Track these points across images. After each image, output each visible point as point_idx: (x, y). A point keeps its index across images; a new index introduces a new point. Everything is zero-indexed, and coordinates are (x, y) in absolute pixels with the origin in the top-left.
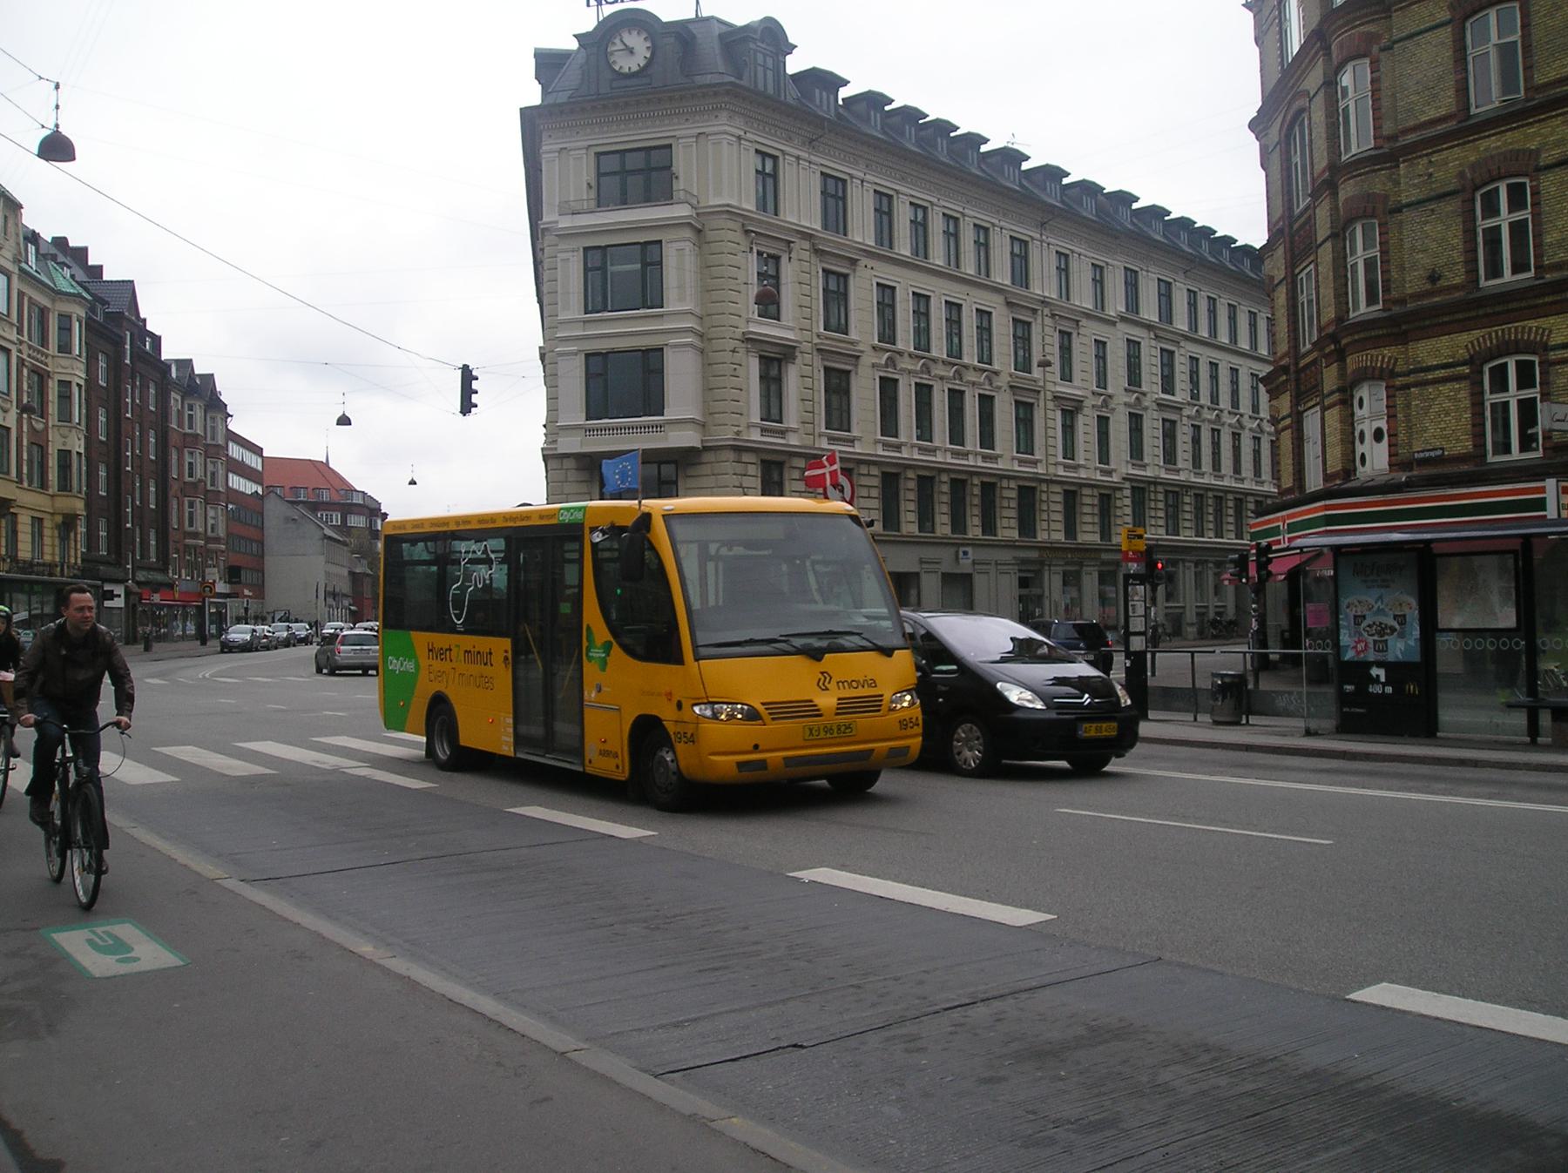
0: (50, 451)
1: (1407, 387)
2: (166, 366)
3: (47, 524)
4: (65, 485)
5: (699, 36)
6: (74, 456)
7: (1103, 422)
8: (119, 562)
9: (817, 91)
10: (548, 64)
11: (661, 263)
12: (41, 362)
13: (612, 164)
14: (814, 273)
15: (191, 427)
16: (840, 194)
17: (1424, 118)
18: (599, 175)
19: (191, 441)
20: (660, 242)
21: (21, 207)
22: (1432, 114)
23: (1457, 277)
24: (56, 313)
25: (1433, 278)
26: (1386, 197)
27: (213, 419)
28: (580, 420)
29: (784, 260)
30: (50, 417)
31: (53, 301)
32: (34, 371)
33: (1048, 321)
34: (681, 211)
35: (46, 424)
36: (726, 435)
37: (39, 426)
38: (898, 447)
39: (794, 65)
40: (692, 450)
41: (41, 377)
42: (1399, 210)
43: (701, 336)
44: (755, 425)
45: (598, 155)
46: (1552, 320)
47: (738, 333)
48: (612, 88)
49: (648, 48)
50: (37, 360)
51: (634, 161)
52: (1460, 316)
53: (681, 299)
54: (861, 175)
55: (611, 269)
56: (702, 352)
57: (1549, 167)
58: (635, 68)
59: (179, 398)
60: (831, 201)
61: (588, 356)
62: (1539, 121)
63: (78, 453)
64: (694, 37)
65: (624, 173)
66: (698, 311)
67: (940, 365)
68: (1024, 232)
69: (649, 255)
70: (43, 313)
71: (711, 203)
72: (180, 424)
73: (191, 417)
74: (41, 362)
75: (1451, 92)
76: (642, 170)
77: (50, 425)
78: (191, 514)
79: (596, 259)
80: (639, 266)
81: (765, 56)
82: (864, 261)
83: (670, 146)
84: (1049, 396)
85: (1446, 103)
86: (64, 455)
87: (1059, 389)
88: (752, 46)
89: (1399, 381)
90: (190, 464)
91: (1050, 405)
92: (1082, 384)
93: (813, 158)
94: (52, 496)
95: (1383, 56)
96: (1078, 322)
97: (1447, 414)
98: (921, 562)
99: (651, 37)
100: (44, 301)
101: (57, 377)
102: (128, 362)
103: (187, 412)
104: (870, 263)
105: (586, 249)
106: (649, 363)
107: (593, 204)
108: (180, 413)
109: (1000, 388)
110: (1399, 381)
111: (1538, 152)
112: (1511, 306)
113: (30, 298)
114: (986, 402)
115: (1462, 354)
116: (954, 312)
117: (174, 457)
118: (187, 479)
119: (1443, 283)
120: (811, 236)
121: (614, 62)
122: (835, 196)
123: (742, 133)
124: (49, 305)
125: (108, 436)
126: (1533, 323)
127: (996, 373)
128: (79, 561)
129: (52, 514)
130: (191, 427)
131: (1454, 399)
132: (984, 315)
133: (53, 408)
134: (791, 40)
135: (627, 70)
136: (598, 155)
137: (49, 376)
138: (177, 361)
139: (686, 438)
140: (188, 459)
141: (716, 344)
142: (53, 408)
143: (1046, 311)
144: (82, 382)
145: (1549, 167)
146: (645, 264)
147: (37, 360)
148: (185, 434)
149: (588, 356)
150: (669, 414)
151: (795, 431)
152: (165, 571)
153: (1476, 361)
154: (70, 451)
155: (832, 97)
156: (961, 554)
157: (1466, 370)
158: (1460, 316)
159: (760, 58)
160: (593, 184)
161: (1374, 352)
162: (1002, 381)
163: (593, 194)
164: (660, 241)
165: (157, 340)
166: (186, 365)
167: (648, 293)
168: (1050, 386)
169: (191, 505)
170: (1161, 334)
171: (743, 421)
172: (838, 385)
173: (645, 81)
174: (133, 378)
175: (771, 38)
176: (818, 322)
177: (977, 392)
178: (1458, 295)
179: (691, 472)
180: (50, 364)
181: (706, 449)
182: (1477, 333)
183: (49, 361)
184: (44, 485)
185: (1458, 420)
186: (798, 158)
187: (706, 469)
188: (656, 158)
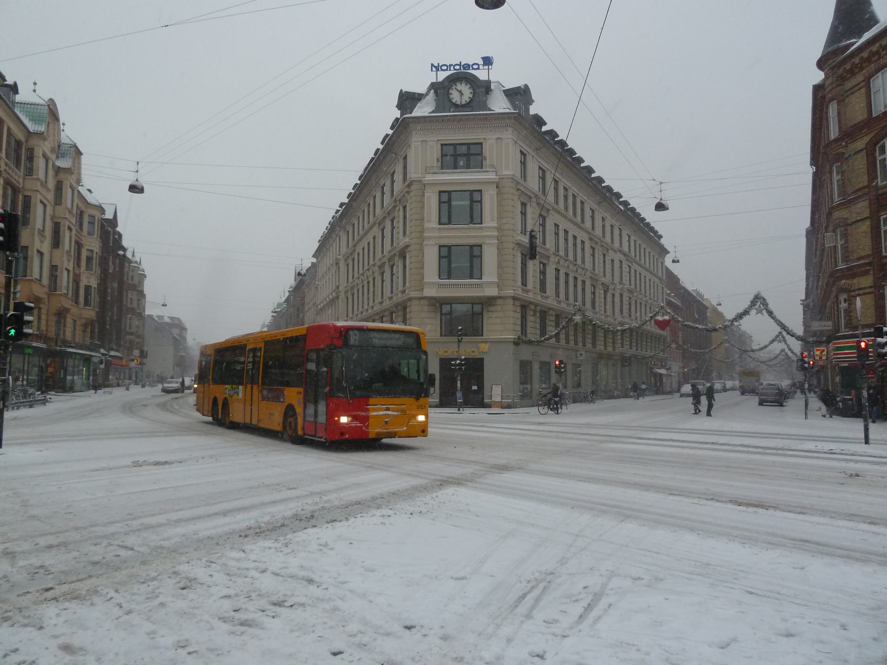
3: (78, 323)
4: (87, 303)
6: (93, 289)
7: (613, 295)
12: (80, 239)
13: (450, 150)
20: (481, 191)
21: (81, 154)
24: (88, 214)
28: (436, 279)
29: (528, 206)
33: (600, 249)
34: (492, 176)
35: (80, 271)
36: (510, 292)
37: (77, 272)
39: (533, 110)
41: (79, 245)
45: (442, 145)
49: (471, 93)
51: (463, 149)
53: (492, 220)
55: (453, 203)
58: (464, 102)
63: (95, 288)
65: (456, 156)
69: (474, 197)
70: (81, 214)
72: (128, 279)
76: (465, 154)
79: (445, 197)
80: (468, 202)
83: (481, 144)
84: (600, 283)
86: (88, 288)
90: (131, 299)
91: (601, 287)
92: (607, 280)
96: (608, 250)
99: (472, 87)
100: (82, 207)
101: (86, 247)
105: (440, 192)
106: (474, 253)
114: (584, 282)
117: (125, 294)
118: (129, 306)
121: (471, 93)
124: (84, 210)
136: (442, 145)
139: (492, 292)
140: (130, 296)
144: (98, 251)
146: (472, 201)
149: (440, 246)
150: (485, 279)
154: (91, 286)
156: (579, 355)
160: (440, 160)
163: (440, 163)
164: (481, 191)
165: (120, 236)
167: (474, 216)
170: (629, 258)
179: (491, 309)
180: (83, 240)
181: (500, 298)
184: (77, 302)
187: (499, 308)
188: (474, 149)
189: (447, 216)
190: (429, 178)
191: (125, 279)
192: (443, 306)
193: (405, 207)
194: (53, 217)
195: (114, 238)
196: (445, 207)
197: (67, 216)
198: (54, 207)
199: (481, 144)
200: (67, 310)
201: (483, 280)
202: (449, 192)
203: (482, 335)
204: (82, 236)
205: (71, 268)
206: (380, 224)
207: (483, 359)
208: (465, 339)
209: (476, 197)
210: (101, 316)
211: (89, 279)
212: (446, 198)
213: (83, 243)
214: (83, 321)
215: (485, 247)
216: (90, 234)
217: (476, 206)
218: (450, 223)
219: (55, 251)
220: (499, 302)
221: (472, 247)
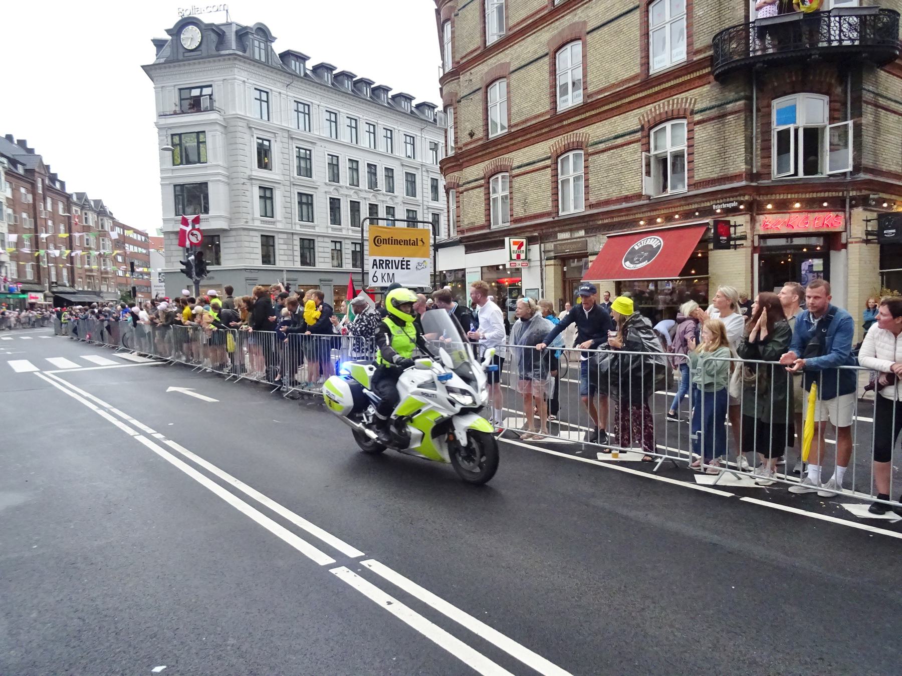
1: (462, 193)
2: (68, 197)
5: (227, 34)
8: (39, 283)
9: (293, 62)
10: (159, 44)
11: (204, 142)
14: (290, 148)
15: (86, 222)
16: (307, 112)
17: (469, 50)
18: (181, 99)
20: (204, 132)
22: (472, 48)
23: (479, 134)
25: (471, 135)
26: (457, 94)
27: (102, 220)
33: (424, 174)
36: (241, 224)
38: (341, 230)
39: (278, 48)
40: (224, 230)
42: (459, 101)
43: (228, 177)
44: (257, 219)
46: (514, 153)
47: (246, 176)
52: (480, 154)
54: (318, 103)
56: (228, 184)
57: (513, 72)
58: (194, 47)
60: (301, 115)
61: (175, 186)
62: (510, 47)
64: (224, 32)
66: (225, 165)
67: (345, 189)
68: (411, 132)
71: (231, 113)
73: (86, 219)
75: (478, 35)
81: (259, 42)
82: (319, 143)
84: (425, 207)
85: (477, 42)
87: (430, 204)
88: (250, 36)
89: (461, 189)
90: (87, 240)
93: (289, 93)
95: (456, 18)
97: (476, 205)
98: (321, 280)
102: (40, 192)
104: (324, 144)
105: (172, 135)
109: (398, 203)
110: (461, 189)
111: (509, 63)
112: (499, 147)
115: (482, 175)
116: (355, 165)
118: (86, 246)
119: (475, 137)
120: (288, 131)
122: (304, 113)
123: (246, 80)
126: (506, 156)
127: (396, 197)
130: (86, 222)
131: (477, 197)
132: (389, 171)
134: (273, 35)
136: (180, 89)
138: (76, 193)
141: (235, 181)
143: (424, 169)
145: (513, 72)
146: (199, 143)
148: (83, 226)
149: (175, 186)
151: (280, 222)
152: (72, 286)
153: (488, 178)
155: (302, 65)
157: (482, 182)
158: (480, 154)
159: (256, 43)
160: (178, 103)
161: (451, 174)
162: (399, 200)
165: (62, 184)
166: (81, 196)
168: (425, 203)
171: (249, 217)
172: (306, 202)
174: (44, 199)
175: (263, 32)
176: (293, 171)
177: (385, 205)
178: (480, 143)
181: (231, 230)
182: (487, 162)
185: (480, 208)
186: (280, 93)
187: (232, 239)
202: (180, 135)
203: (218, 263)
215: (210, 186)
218: (181, 163)
220: (233, 233)
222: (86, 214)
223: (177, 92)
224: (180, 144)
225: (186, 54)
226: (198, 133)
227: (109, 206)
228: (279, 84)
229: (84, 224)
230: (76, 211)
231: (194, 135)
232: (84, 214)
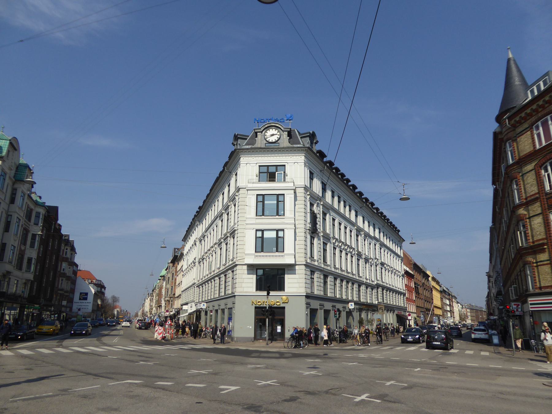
0: (25, 257)
12: (28, 227)
13: (265, 169)
18: (260, 173)
19: (66, 260)
20: (284, 195)
30: (27, 246)
31: (35, 207)
32: (25, 229)
35: (25, 248)
37: (23, 248)
41: (26, 231)
45: (260, 166)
48: (265, 146)
50: (27, 226)
55: (266, 202)
58: (274, 141)
59: (64, 245)
61: (256, 230)
69: (279, 198)
72: (63, 254)
73: (66, 252)
74: (28, 227)
77: (26, 248)
78: (62, 283)
79: (260, 199)
83: (285, 165)
86: (30, 260)
94: (23, 273)
100: (32, 206)
101: (32, 232)
103: (65, 250)
105: (257, 195)
107: (258, 180)
108: (63, 251)
113: (28, 205)
125: (42, 255)
128: (27, 296)
129: (22, 279)
133: (29, 243)
135: (271, 141)
136: (260, 166)
137: (29, 232)
142: (29, 243)
146: (278, 201)
147: (27, 226)
149: (256, 230)
160: (258, 175)
163: (258, 178)
167: (279, 211)
169: (62, 280)
173: (278, 144)
183: (30, 227)
189: (261, 211)
190: (250, 186)
191: (61, 254)
192: (258, 270)
193: (235, 205)
194: (7, 212)
195: (55, 227)
196: (260, 204)
197: (17, 210)
198: (9, 206)
199: (285, 165)
200: (9, 273)
201: (285, 253)
202: (263, 195)
203: (284, 290)
204: (30, 225)
205: (16, 245)
206: (220, 217)
207: (284, 308)
208: (272, 293)
209: (281, 198)
210: (39, 278)
211: (32, 253)
212: (261, 199)
213: (30, 229)
214: (24, 281)
216: (36, 224)
217: (281, 204)
219: (6, 233)
221: (277, 231)
222: (67, 249)
223: (258, 167)
224: (263, 202)
225: (267, 145)
226: (278, 195)
227: (76, 245)
228: (318, 170)
229: (64, 256)
230: (63, 246)
231: (275, 197)
232: (65, 249)
